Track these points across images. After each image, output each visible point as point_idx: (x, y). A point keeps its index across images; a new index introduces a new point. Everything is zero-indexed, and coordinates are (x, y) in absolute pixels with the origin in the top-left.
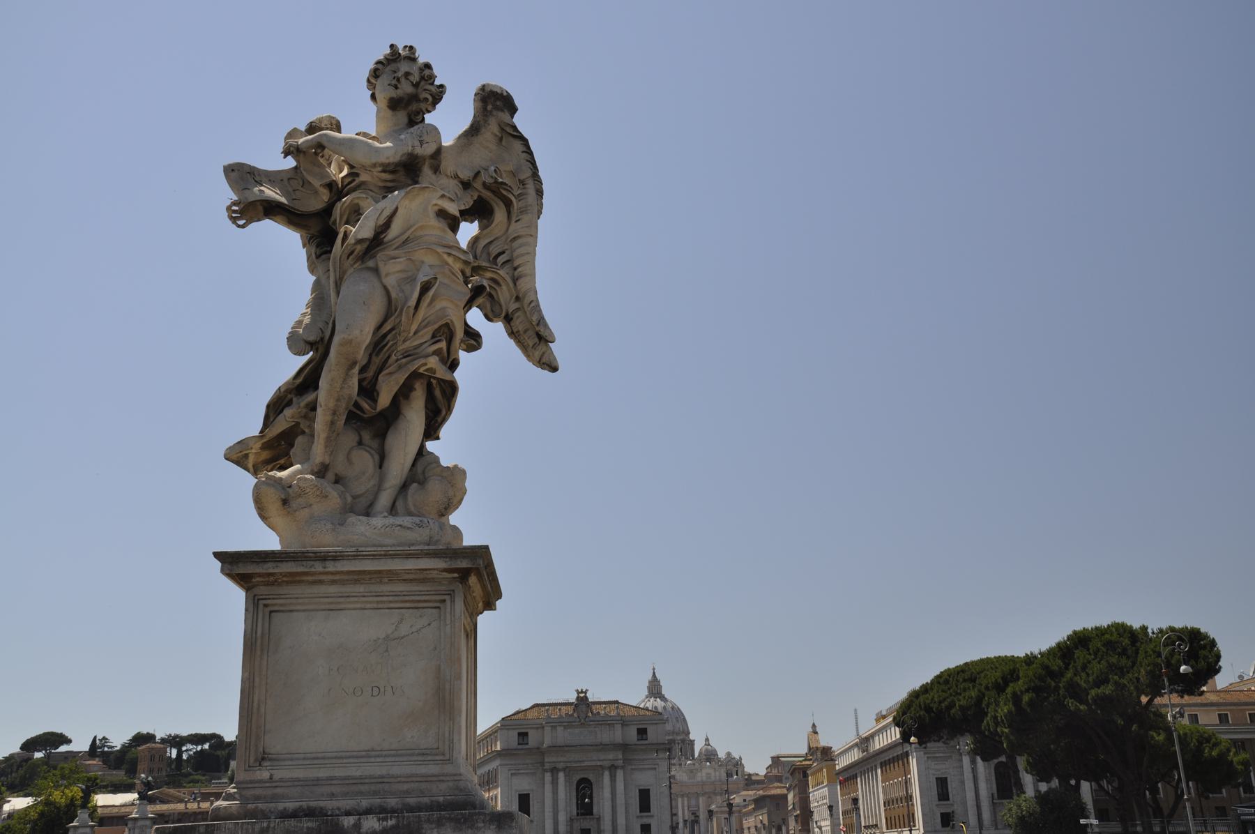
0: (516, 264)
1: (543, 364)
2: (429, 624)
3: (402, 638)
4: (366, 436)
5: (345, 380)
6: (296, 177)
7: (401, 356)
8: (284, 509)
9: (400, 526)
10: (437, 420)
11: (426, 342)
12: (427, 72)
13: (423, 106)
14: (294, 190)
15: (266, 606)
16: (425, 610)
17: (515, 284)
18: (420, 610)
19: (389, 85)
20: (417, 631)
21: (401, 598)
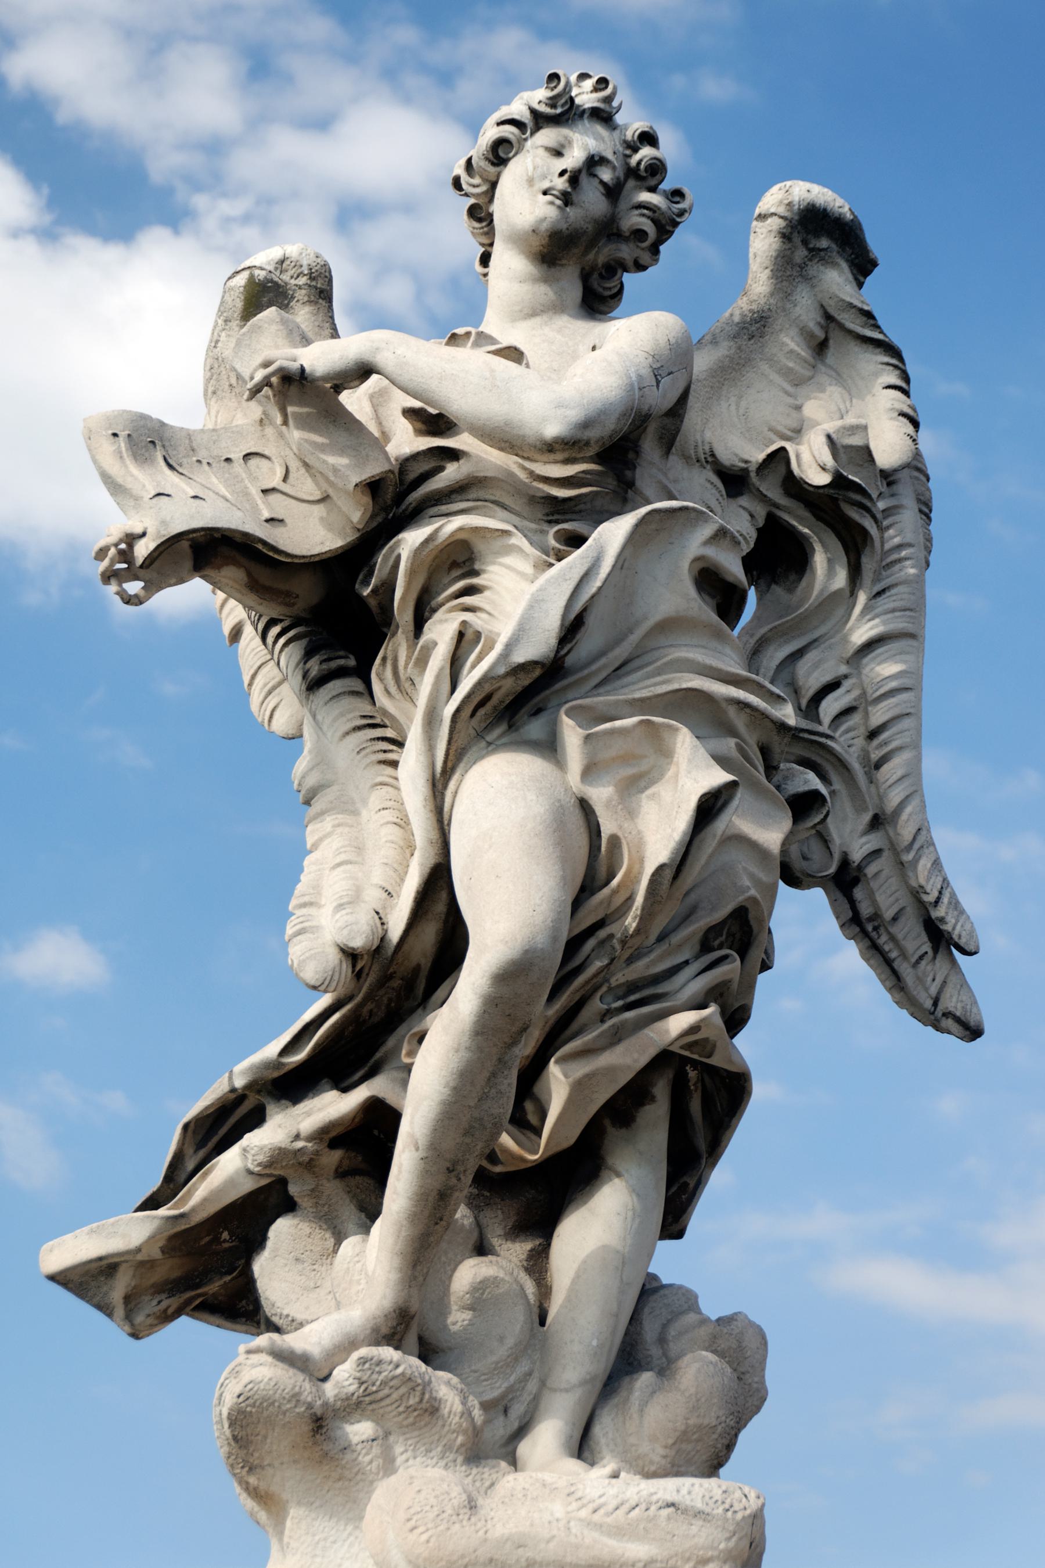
0: (878, 715)
1: (947, 1014)
5: (494, 1075)
7: (620, 1003)
8: (315, 1443)
9: (673, 1505)
10: (686, 1184)
11: (686, 963)
13: (626, 252)
14: (265, 492)
19: (545, 193)
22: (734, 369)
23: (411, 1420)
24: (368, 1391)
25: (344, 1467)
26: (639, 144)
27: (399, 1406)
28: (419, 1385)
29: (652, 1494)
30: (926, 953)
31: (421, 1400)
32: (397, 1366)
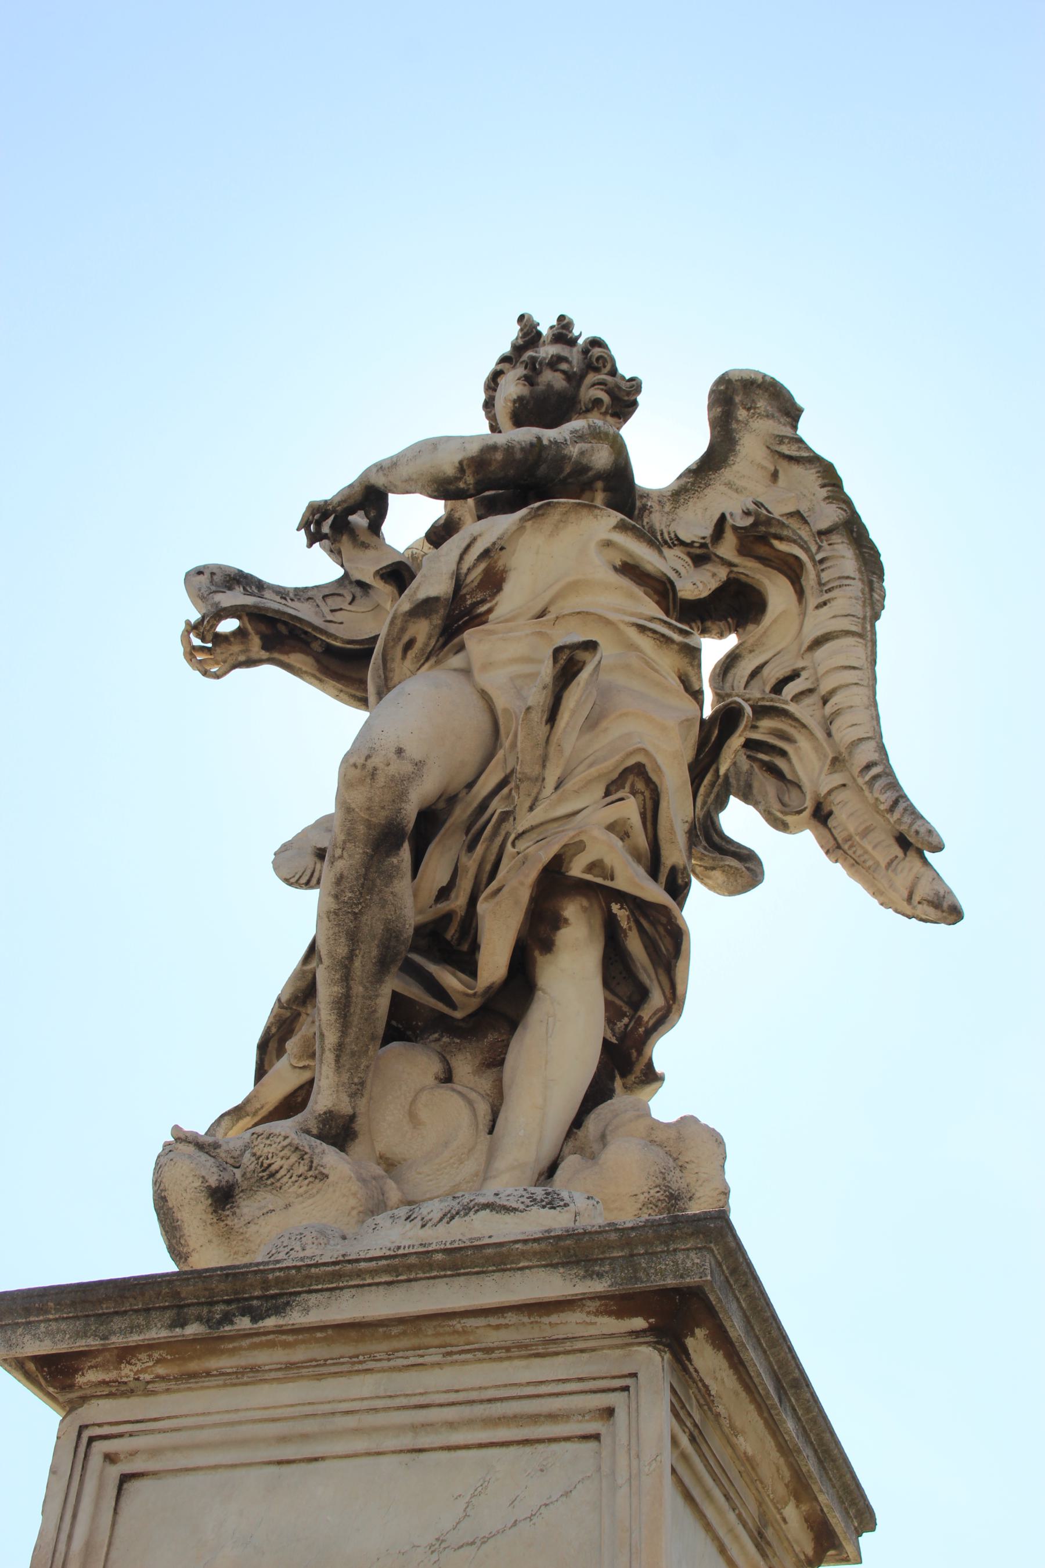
2: (567, 1494)
3: (485, 1541)
4: (464, 1066)
6: (341, 592)
8: (220, 1219)
10: (640, 1018)
12: (596, 351)
15: (110, 1458)
16: (554, 1447)
17: (829, 734)
18: (540, 1447)
20: (530, 1518)
21: (479, 1410)
22: (697, 491)
23: (304, 1188)
24: (265, 1165)
25: (248, 1240)
26: (590, 348)
27: (291, 1177)
28: (306, 1153)
29: (471, 1201)
30: (896, 857)
31: (310, 1168)
32: (286, 1138)
